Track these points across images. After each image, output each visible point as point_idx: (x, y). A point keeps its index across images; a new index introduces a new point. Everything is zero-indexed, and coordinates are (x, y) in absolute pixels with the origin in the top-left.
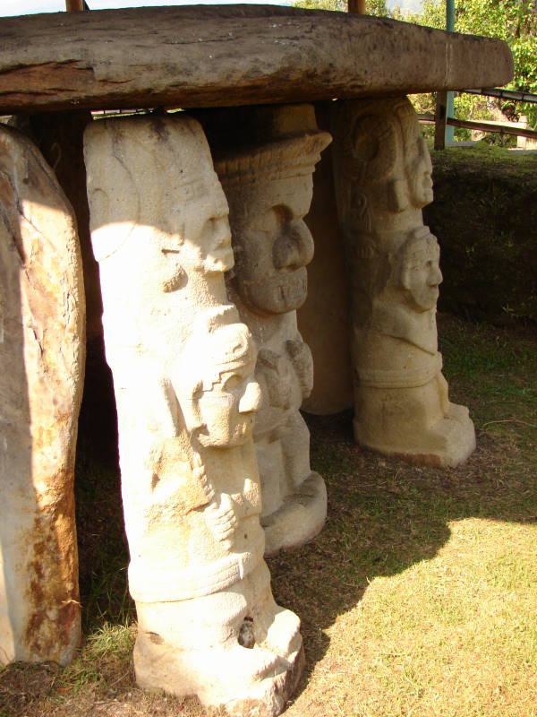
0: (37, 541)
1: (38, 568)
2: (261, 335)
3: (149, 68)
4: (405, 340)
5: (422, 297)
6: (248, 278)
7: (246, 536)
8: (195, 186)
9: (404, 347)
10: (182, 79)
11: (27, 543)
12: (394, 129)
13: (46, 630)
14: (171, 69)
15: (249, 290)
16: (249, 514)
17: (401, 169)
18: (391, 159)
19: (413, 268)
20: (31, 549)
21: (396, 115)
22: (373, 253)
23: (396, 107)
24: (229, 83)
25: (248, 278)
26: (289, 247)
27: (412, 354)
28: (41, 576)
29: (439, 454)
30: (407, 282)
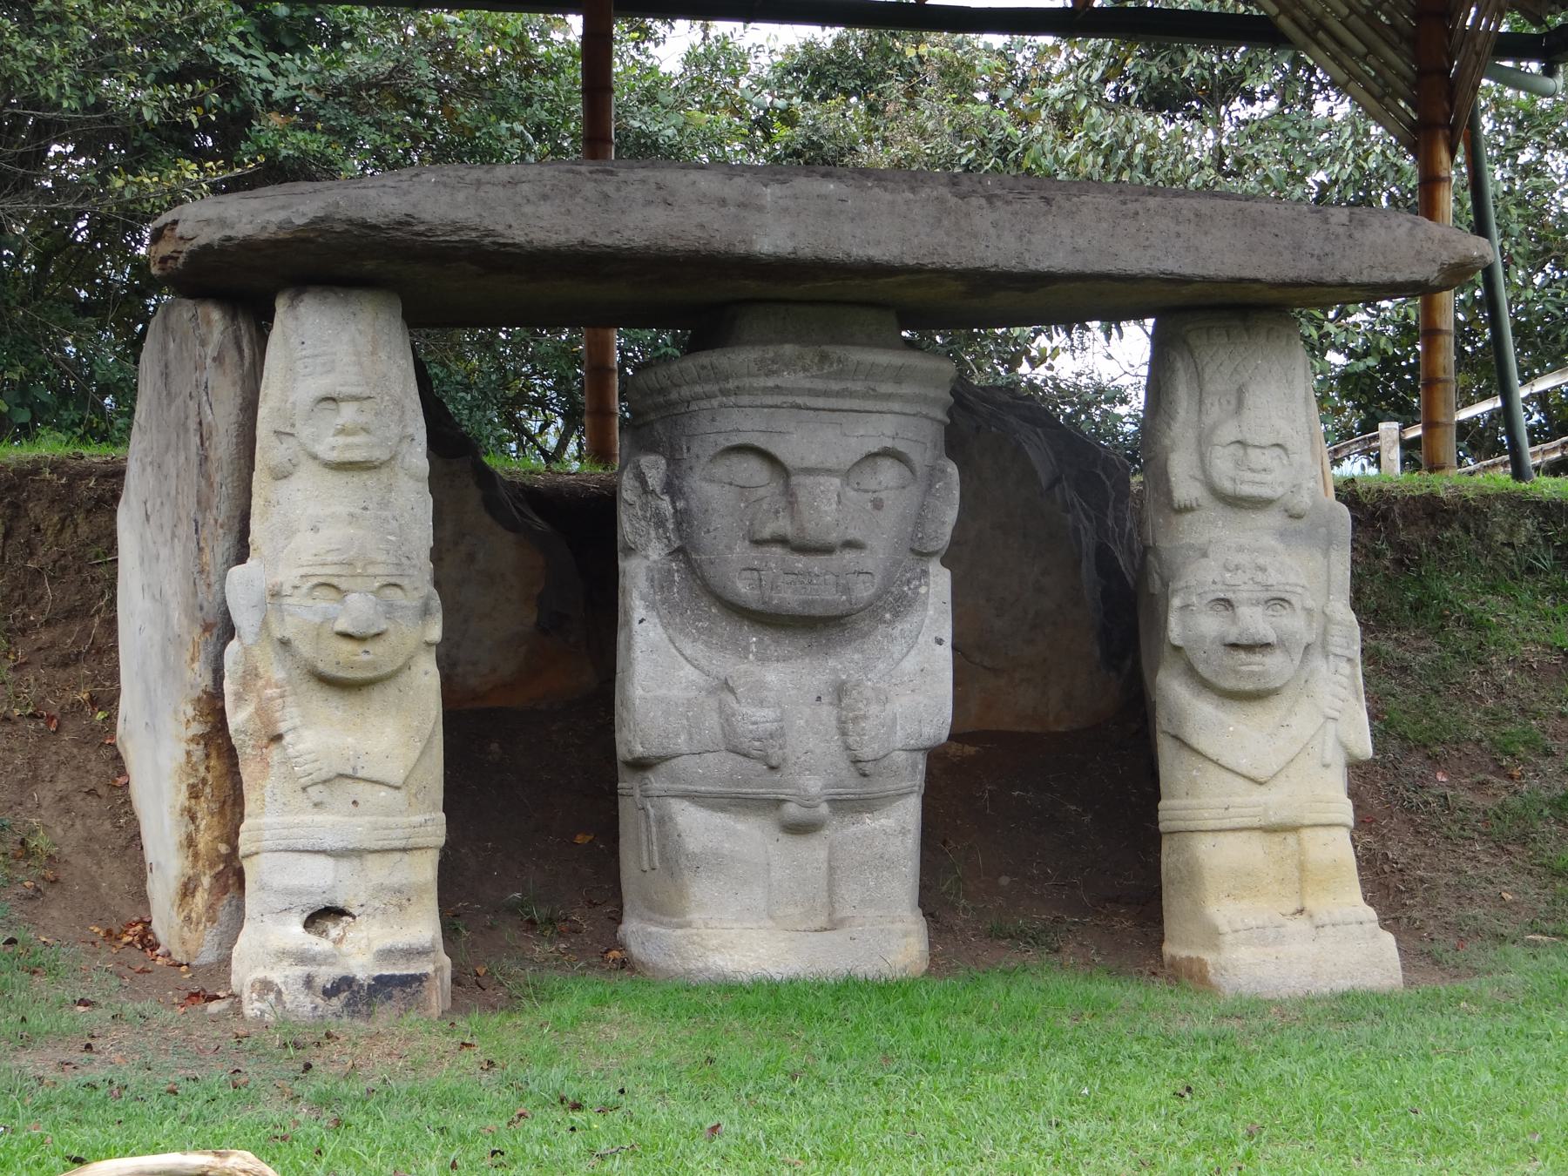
0: (191, 781)
1: (193, 818)
3: (208, 222)
4: (1182, 742)
5: (1206, 661)
6: (697, 551)
8: (320, 360)
9: (1185, 755)
10: (228, 232)
11: (181, 781)
12: (1179, 365)
13: (200, 899)
14: (223, 222)
15: (700, 566)
16: (359, 775)
17: (1191, 435)
18: (1172, 417)
19: (1185, 607)
20: (184, 787)
21: (1185, 342)
22: (1158, 583)
23: (1189, 327)
24: (265, 235)
25: (697, 551)
26: (777, 512)
27: (1199, 770)
28: (197, 829)
29: (1209, 957)
30: (1175, 630)
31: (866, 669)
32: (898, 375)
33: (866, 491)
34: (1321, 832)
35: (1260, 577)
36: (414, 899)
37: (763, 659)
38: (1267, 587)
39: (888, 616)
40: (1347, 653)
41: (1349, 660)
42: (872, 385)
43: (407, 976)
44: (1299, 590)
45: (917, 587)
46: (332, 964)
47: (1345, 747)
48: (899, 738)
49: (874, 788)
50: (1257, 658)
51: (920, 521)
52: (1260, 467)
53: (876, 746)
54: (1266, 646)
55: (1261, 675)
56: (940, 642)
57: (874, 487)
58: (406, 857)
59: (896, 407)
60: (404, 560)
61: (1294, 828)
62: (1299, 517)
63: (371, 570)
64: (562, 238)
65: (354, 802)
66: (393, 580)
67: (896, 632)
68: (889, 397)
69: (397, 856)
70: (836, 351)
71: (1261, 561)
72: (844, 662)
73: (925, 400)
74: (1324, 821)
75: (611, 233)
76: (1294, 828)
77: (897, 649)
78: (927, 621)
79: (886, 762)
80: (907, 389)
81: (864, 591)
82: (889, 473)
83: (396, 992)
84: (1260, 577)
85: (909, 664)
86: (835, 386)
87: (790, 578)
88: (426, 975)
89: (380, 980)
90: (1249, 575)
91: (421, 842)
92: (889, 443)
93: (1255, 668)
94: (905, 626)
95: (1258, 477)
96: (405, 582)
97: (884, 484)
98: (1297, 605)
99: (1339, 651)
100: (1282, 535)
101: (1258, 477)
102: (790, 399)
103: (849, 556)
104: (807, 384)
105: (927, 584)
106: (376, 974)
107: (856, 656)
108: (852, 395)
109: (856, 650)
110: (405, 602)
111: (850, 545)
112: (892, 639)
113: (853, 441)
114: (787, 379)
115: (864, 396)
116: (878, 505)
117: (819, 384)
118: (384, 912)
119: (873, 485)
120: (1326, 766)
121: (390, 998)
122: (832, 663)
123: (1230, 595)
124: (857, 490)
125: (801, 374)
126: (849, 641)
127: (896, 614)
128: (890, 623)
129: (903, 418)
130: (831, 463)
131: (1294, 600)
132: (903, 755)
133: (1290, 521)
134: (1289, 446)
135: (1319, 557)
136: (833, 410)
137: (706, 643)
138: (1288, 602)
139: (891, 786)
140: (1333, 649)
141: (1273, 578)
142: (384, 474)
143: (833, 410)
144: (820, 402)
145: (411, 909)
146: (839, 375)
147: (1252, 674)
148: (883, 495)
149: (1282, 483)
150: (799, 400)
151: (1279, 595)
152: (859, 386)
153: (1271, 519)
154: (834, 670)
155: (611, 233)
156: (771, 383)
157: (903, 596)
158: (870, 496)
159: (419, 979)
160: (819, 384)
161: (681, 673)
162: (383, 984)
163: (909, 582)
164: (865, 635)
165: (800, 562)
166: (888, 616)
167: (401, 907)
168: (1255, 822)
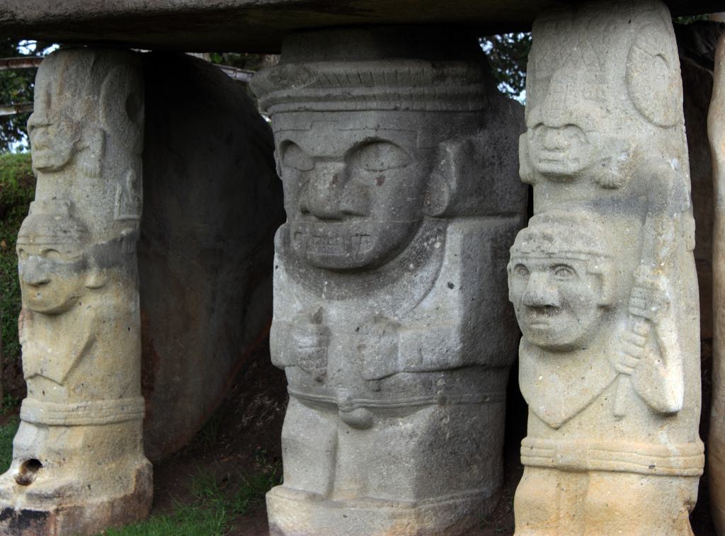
2: (325, 290)
7: (44, 392)
31: (394, 307)
32: (362, 80)
33: (375, 171)
34: (608, 478)
35: (546, 245)
36: (67, 459)
37: (330, 298)
38: (550, 255)
39: (411, 266)
40: (643, 313)
41: (647, 320)
42: (347, 89)
43: (37, 512)
44: (583, 257)
45: (434, 243)
46: (8, 499)
47: (643, 400)
48: (401, 362)
49: (388, 400)
50: (543, 318)
51: (423, 189)
52: (551, 146)
53: (372, 370)
54: (548, 306)
55: (548, 333)
56: (451, 286)
57: (379, 168)
58: (69, 431)
59: (374, 105)
60: (60, 234)
61: (585, 471)
62: (614, 188)
63: (38, 240)
64: (37, 12)
65: (44, 392)
66: (49, 247)
67: (417, 279)
68: (364, 98)
69: (63, 429)
70: (312, 67)
71: (549, 231)
72: (381, 300)
73: (421, 97)
74: (605, 467)
75: (57, 6)
76: (585, 471)
77: (418, 292)
78: (443, 270)
79: (392, 380)
80: (377, 91)
81: (367, 249)
82: (387, 158)
83: (32, 522)
84: (546, 245)
85: (428, 304)
86: (322, 93)
87: (316, 240)
88: (48, 513)
89: (24, 512)
90: (537, 244)
91: (73, 421)
92: (372, 134)
93: (542, 327)
94: (426, 273)
95: (552, 155)
96: (59, 248)
97: (386, 165)
98: (581, 269)
99: (636, 311)
100: (596, 205)
101: (552, 155)
102: (302, 105)
103: (356, 222)
104: (305, 93)
105: (443, 242)
106: (23, 508)
107: (388, 297)
108: (335, 99)
109: (388, 293)
110: (62, 262)
111: (348, 214)
112: (414, 284)
113: (345, 134)
114: (295, 90)
115: (344, 98)
116: (380, 181)
117: (312, 92)
118: (53, 467)
119: (377, 166)
120: (619, 418)
121: (29, 525)
122: (371, 302)
123: (524, 262)
124: (368, 170)
125: (303, 86)
126: (383, 286)
127: (418, 265)
128: (413, 272)
129: (384, 114)
130: (330, 152)
131: (576, 265)
132: (410, 376)
133: (602, 191)
134: (581, 124)
135: (638, 223)
136: (333, 111)
137: (303, 284)
138: (571, 267)
139: (403, 399)
140: (631, 309)
141: (557, 246)
142: (68, 174)
143: (333, 111)
144: (321, 106)
145: (65, 466)
146: (320, 84)
147: (540, 332)
148: (386, 173)
149: (577, 160)
150: (308, 105)
151: (561, 261)
152: (337, 92)
153: (581, 191)
154: (372, 308)
155: (57, 6)
156: (284, 93)
157: (423, 250)
158: (377, 174)
159: (44, 515)
160: (312, 92)
161: (294, 306)
162: (27, 516)
163: (428, 239)
164: (394, 281)
165: (322, 228)
166: (411, 266)
167: (60, 463)
168: (549, 462)
